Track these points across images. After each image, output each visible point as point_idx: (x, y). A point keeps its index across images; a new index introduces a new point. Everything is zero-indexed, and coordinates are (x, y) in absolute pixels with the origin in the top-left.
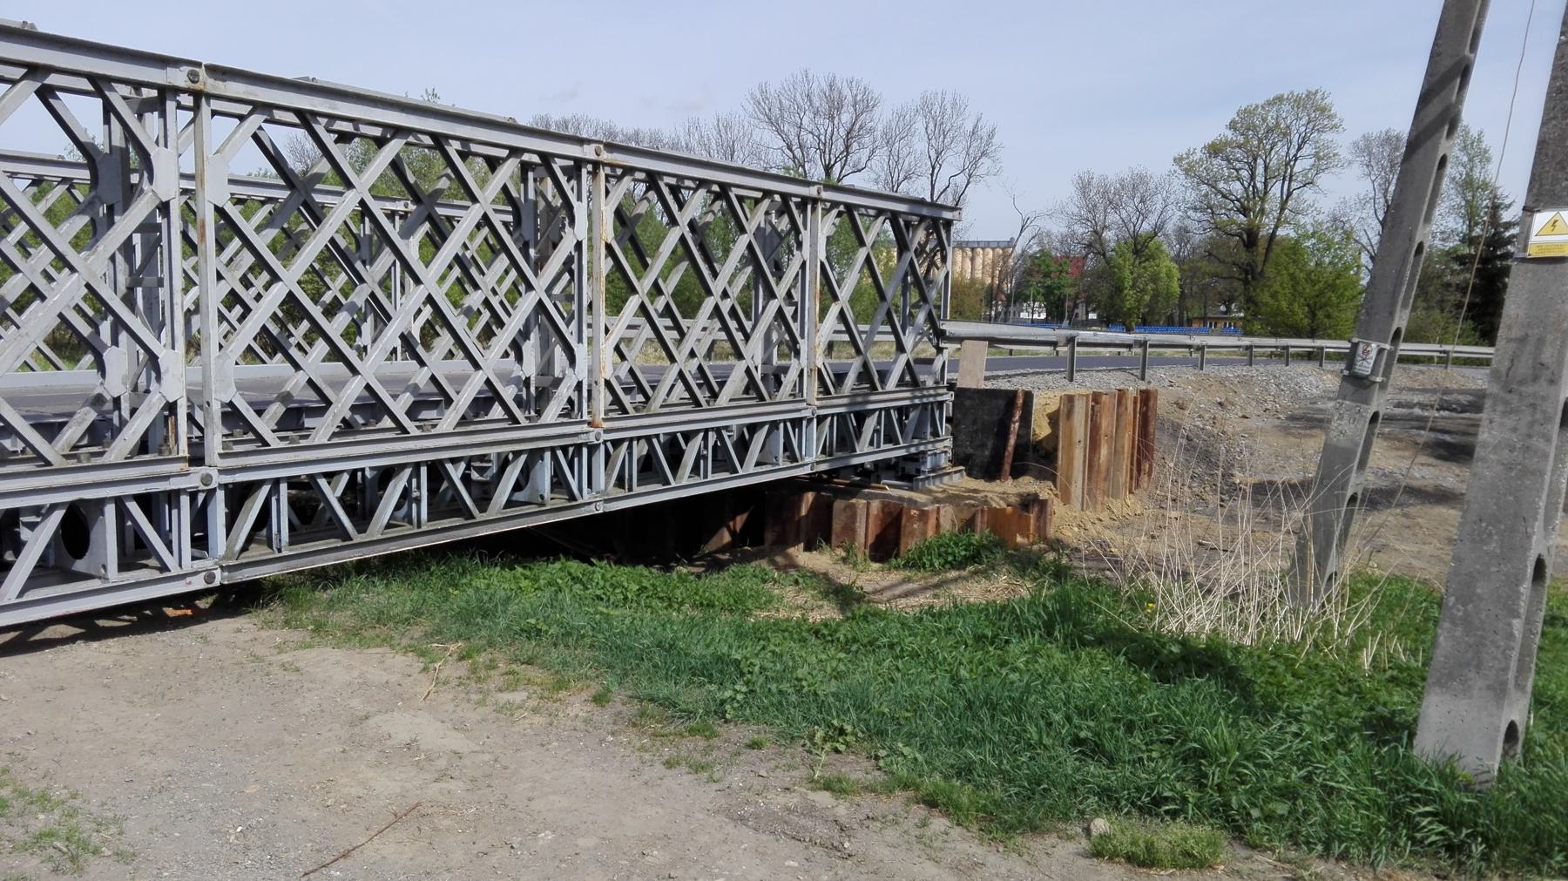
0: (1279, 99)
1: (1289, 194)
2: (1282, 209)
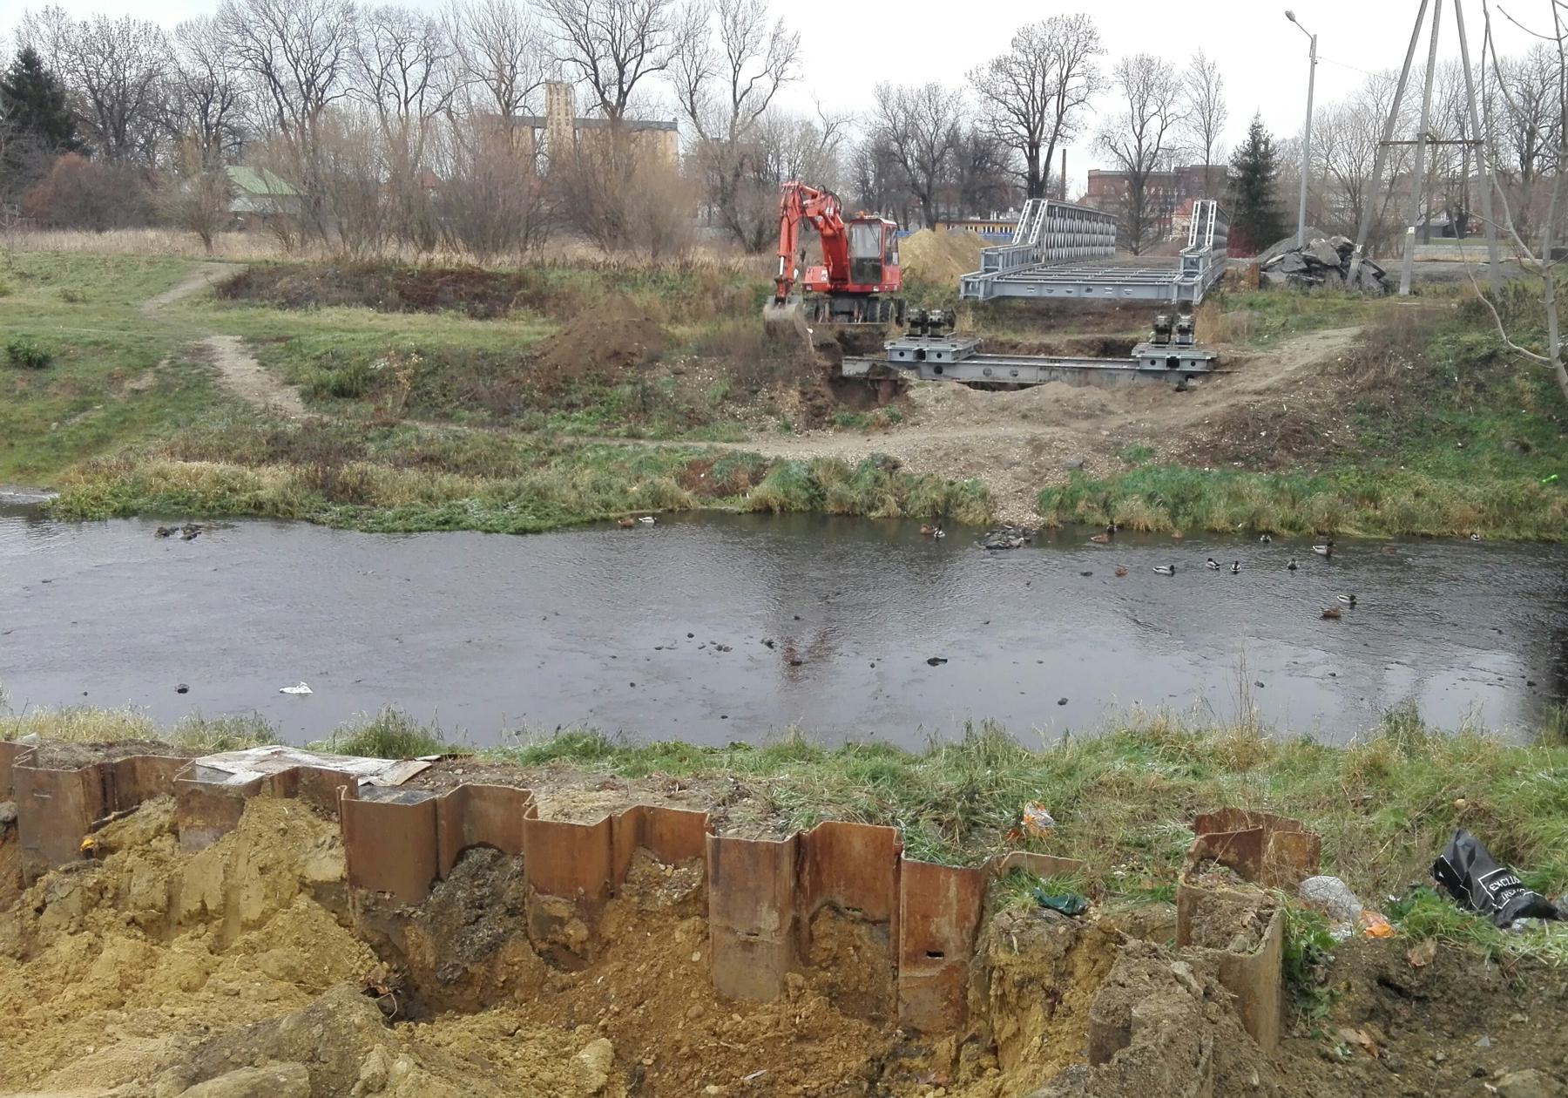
1: (1062, 112)
2: (1059, 122)
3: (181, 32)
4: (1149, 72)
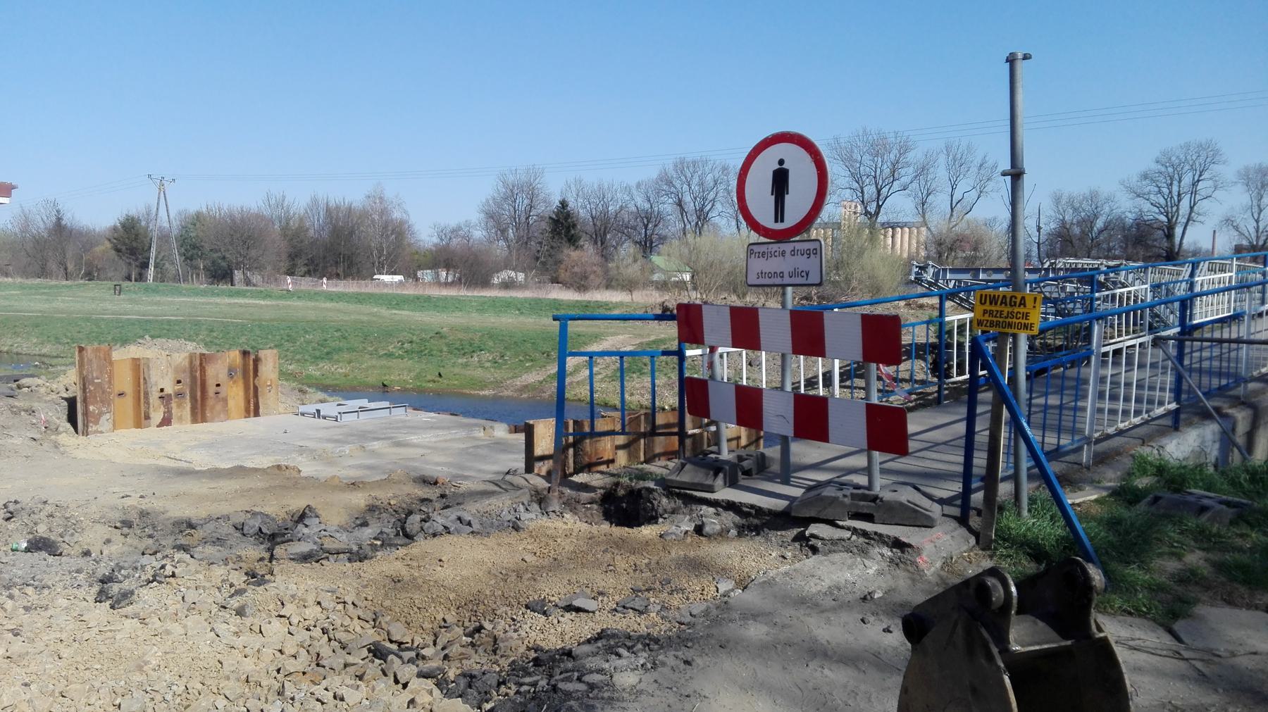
0: (1187, 146)
1: (1194, 205)
3: (638, 185)
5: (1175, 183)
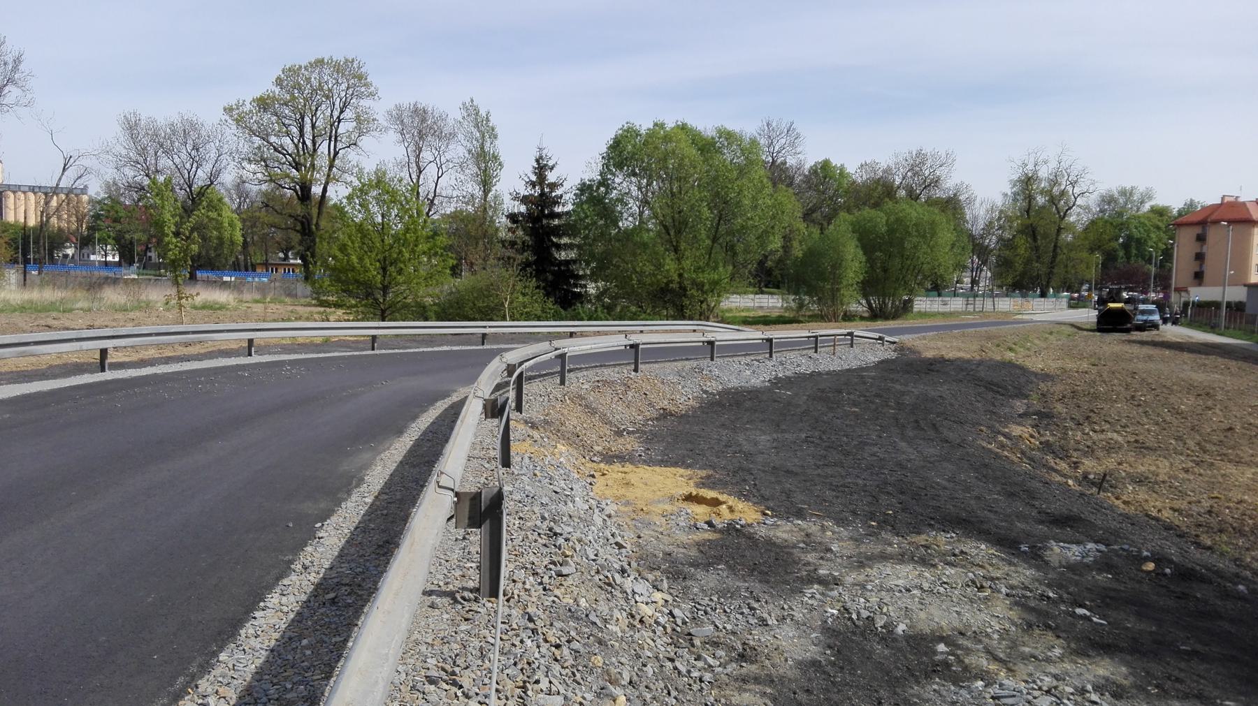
0: (320, 62)
1: (336, 153)
2: (331, 166)
4: (423, 120)
5: (307, 120)
